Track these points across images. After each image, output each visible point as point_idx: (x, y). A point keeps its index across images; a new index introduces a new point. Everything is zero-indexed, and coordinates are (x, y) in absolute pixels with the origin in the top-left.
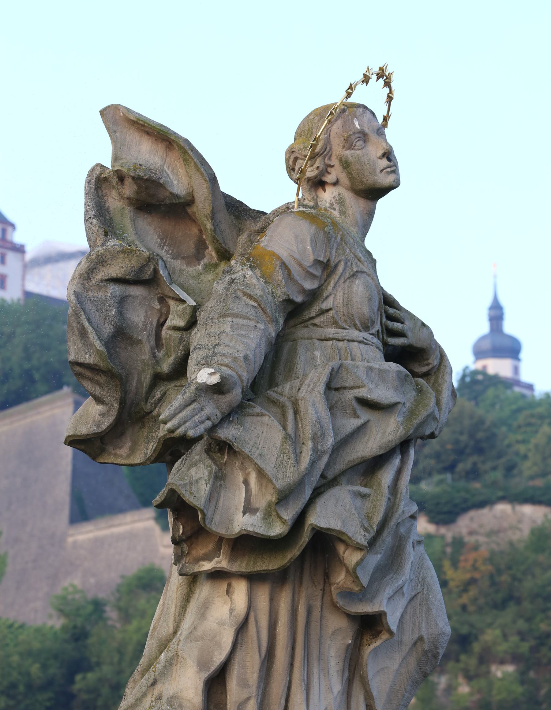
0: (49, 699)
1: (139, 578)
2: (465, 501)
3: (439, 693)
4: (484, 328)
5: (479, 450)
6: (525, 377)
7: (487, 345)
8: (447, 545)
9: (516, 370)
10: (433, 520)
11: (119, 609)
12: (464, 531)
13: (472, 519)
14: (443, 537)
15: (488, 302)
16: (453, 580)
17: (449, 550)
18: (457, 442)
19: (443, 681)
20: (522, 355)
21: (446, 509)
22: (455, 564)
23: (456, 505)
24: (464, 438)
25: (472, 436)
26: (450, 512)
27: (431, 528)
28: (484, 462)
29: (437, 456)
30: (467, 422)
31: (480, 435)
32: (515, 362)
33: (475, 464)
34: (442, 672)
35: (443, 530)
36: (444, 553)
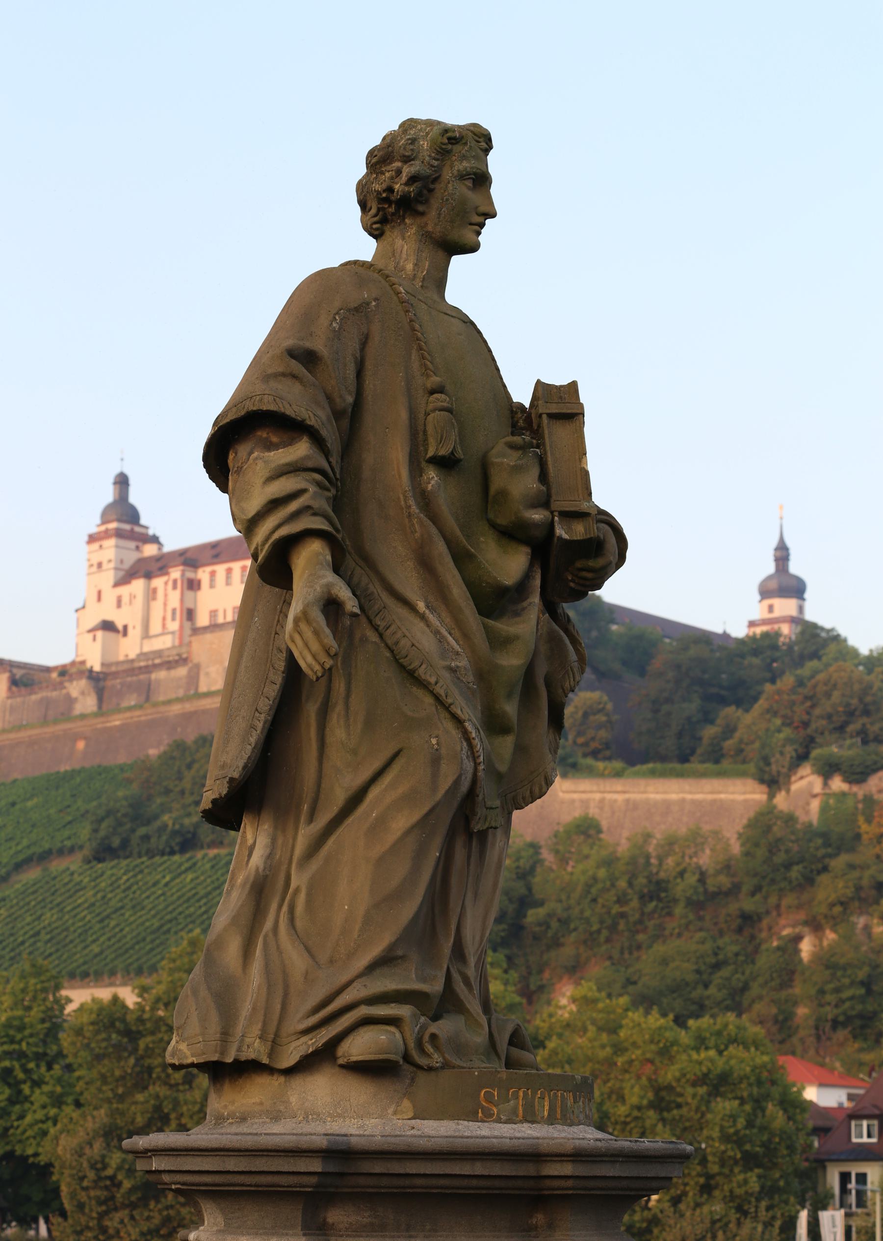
0: (503, 930)
1: (578, 826)
2: (875, 763)
3: (858, 931)
4: (770, 568)
5: (867, 712)
6: (811, 615)
7: (773, 585)
8: (859, 802)
9: (801, 609)
10: (847, 780)
11: (557, 852)
12: (874, 790)
13: (880, 779)
14: (855, 795)
15: (774, 543)
16: (867, 833)
17: (860, 806)
18: (848, 705)
19: (861, 921)
20: (807, 595)
21: (859, 770)
22: (869, 821)
23: (867, 767)
24: (855, 702)
25: (861, 700)
26: (862, 773)
27: (845, 787)
28: (872, 724)
29: (829, 717)
30: (856, 687)
31: (869, 699)
32: (800, 602)
33: (864, 725)
34: (861, 914)
35: (855, 789)
36: (856, 808)
